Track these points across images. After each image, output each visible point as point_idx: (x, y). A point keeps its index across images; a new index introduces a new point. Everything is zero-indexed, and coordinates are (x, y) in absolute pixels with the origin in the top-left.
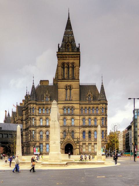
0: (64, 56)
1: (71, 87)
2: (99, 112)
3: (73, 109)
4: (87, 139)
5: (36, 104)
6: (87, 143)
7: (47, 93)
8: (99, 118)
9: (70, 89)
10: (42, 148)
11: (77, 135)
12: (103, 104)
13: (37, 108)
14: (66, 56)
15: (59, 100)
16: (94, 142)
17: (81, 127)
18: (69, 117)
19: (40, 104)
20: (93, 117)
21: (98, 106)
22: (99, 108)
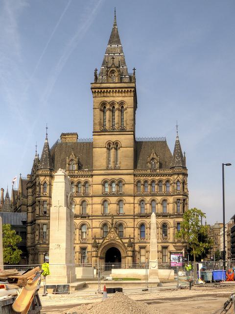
1: (117, 145)
2: (171, 189)
3: (121, 184)
7: (72, 156)
8: (171, 199)
9: (116, 149)
11: (128, 232)
12: (178, 174)
14: (109, 90)
16: (161, 244)
17: (136, 217)
18: (113, 200)
20: (159, 199)
21: (169, 177)
22: (172, 182)
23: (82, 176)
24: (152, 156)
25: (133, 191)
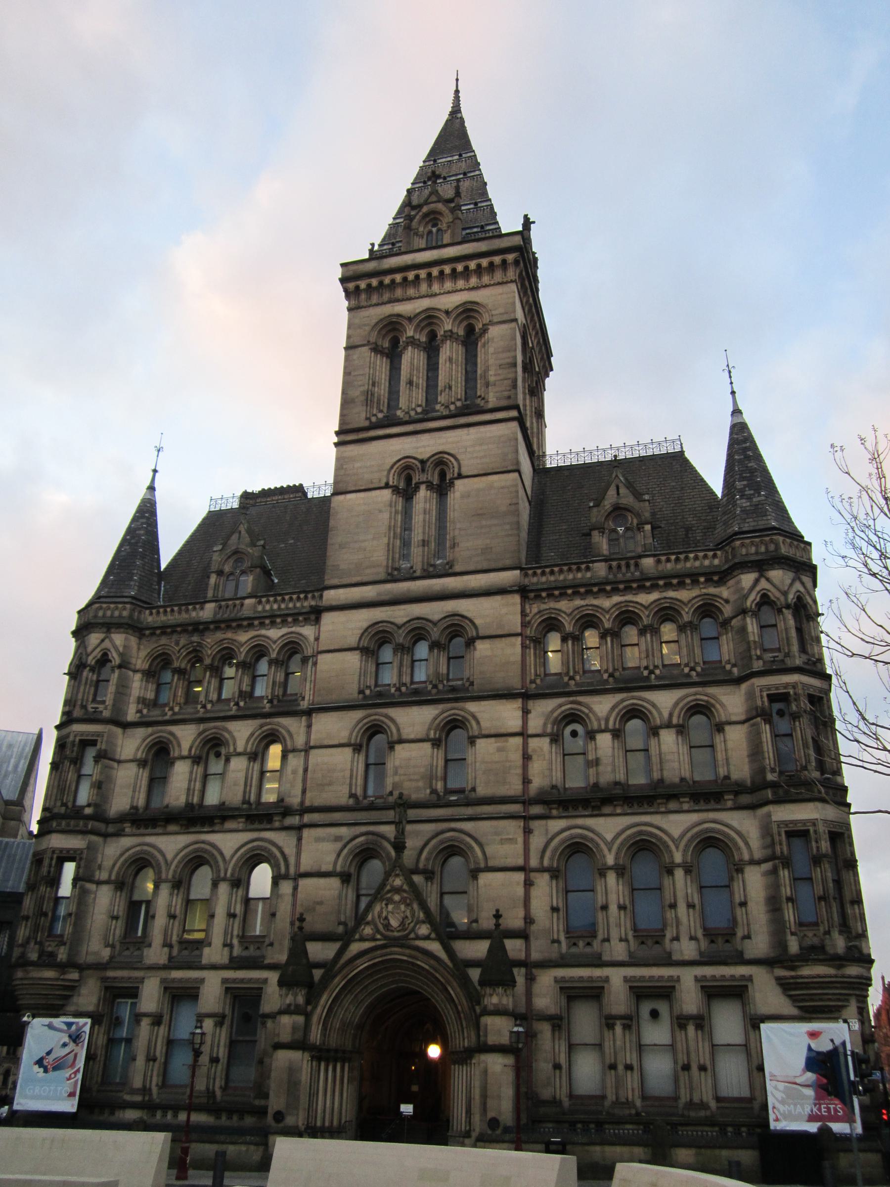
0: (398, 277)
4: (615, 934)
6: (617, 978)
9: (442, 488)
10: (129, 1041)
13: (140, 658)
14: (411, 275)
15: (335, 581)
17: (536, 810)
21: (712, 590)
22: (728, 611)
23: (273, 619)
24: (611, 497)
25: (517, 668)
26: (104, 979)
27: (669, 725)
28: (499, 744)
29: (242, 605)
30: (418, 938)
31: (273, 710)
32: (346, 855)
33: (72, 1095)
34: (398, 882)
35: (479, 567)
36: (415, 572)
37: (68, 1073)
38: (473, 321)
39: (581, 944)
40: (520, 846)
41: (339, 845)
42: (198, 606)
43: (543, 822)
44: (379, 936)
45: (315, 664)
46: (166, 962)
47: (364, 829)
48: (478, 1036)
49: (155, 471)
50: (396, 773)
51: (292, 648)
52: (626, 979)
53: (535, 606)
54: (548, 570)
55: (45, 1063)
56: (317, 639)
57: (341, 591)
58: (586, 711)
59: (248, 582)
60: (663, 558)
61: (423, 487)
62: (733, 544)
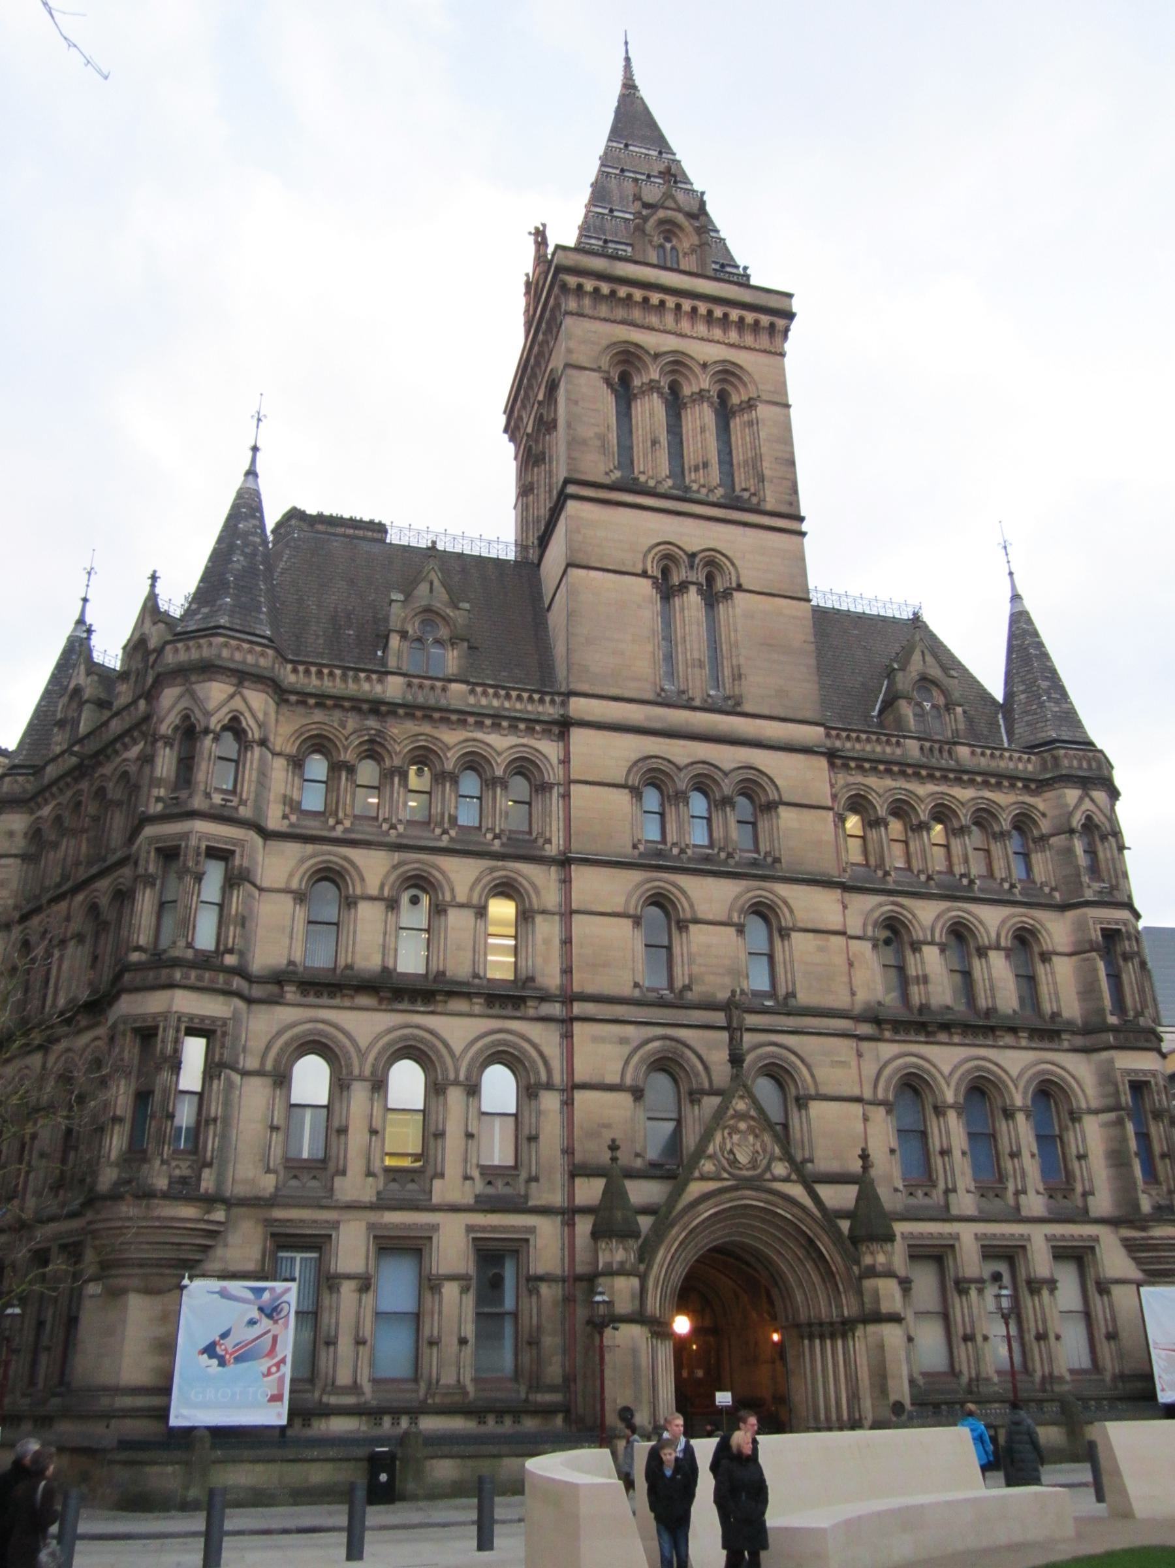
0: (638, 295)
2: (1043, 866)
5: (281, 693)
9: (713, 598)
14: (655, 298)
19: (322, 701)
22: (1045, 826)
23: (497, 720)
26: (268, 1222)
27: (998, 947)
28: (819, 943)
29: (444, 689)
30: (775, 1179)
31: (502, 850)
32: (637, 1064)
33: (276, 1398)
34: (741, 1105)
35: (775, 713)
36: (693, 699)
37: (264, 1364)
38: (681, 380)
39: (920, 1193)
40: (854, 1071)
41: (626, 1050)
42: (374, 676)
43: (872, 1045)
44: (725, 1175)
45: (566, 796)
46: (374, 1199)
47: (660, 1031)
48: (863, 1304)
49: (255, 449)
50: (691, 961)
51: (524, 767)
52: (977, 1237)
53: (840, 776)
54: (854, 735)
55: (219, 1350)
56: (566, 761)
57: (595, 702)
58: (910, 917)
59: (452, 660)
60: (979, 750)
61: (693, 589)
62: (1055, 752)
